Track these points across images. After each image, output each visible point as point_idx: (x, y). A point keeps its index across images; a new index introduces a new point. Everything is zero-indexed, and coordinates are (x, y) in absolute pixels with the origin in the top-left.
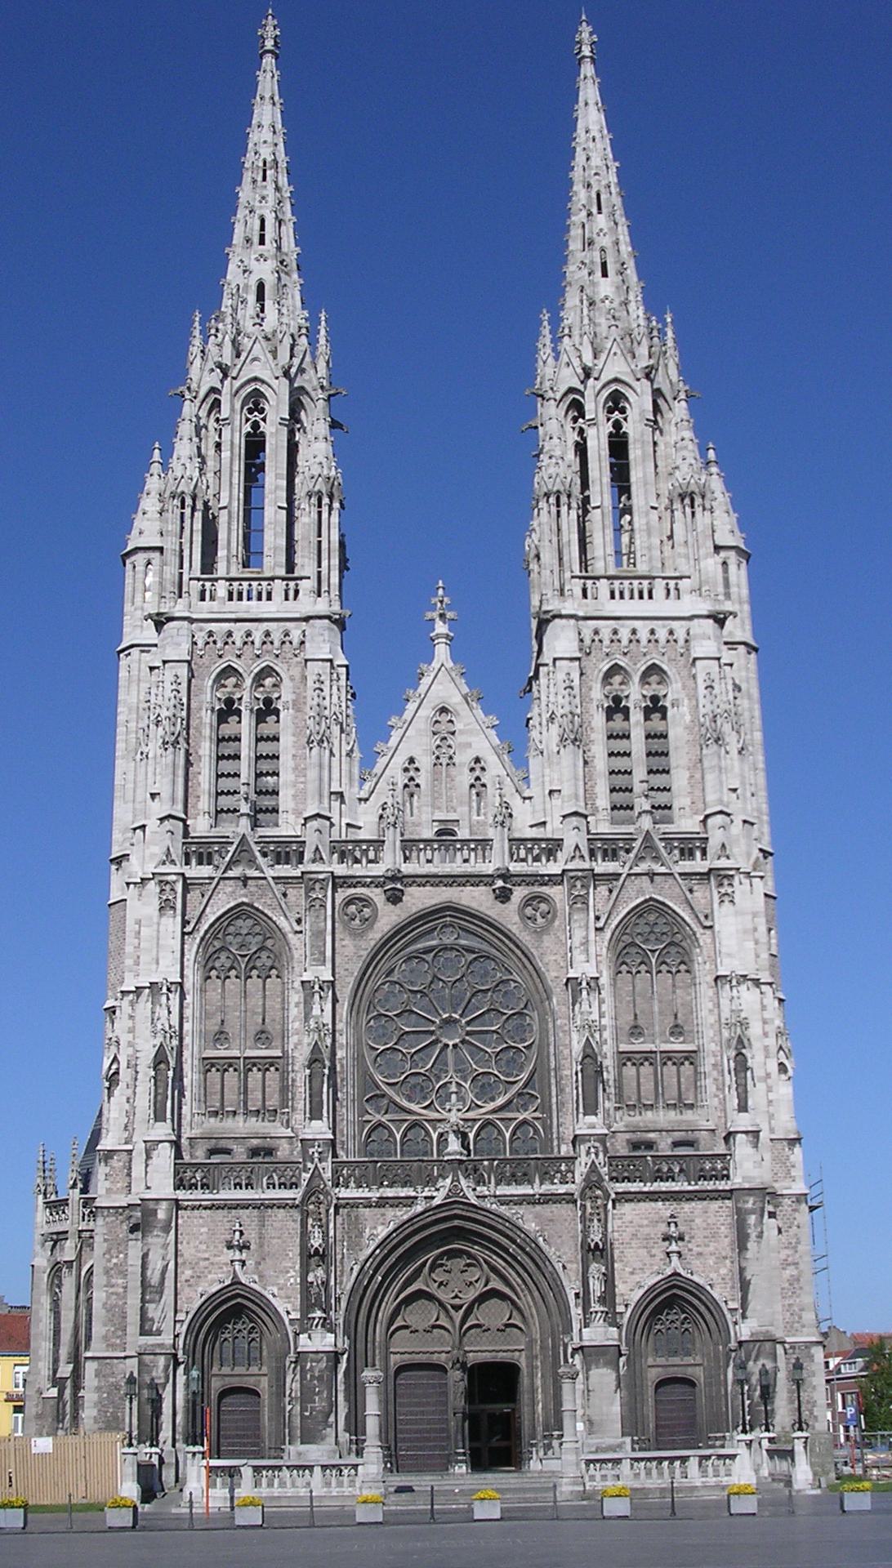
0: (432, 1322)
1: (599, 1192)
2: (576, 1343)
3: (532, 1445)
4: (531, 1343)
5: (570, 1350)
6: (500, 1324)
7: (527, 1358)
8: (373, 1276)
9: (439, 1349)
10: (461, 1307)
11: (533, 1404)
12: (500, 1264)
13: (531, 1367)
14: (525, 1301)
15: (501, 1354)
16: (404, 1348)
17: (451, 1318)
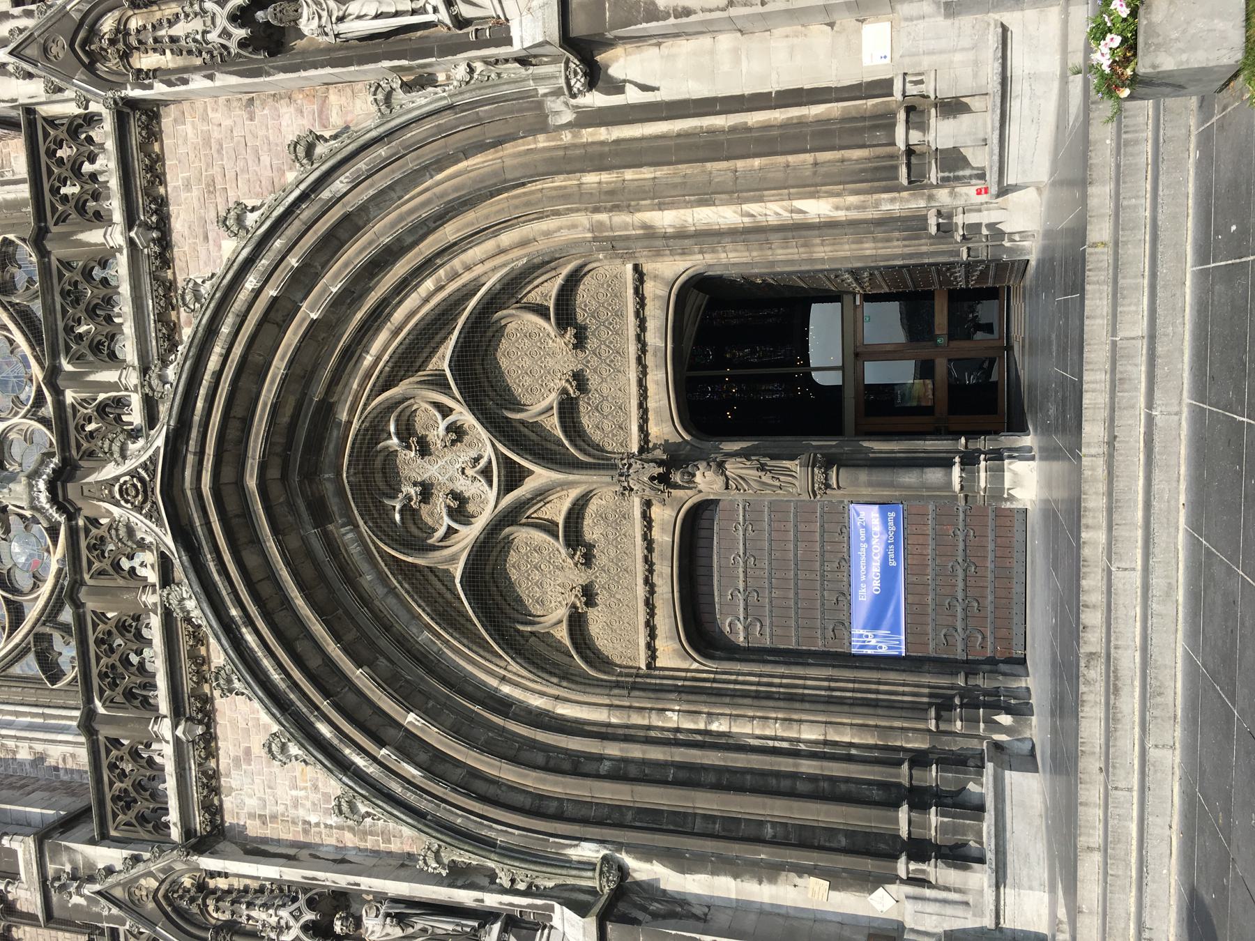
0: (560, 545)
1: (108, 25)
2: (556, 70)
3: (945, 230)
4: (615, 245)
5: (596, 99)
6: (558, 344)
7: (657, 254)
8: (409, 746)
9: (633, 527)
10: (506, 463)
11: (799, 230)
12: (381, 348)
13: (683, 239)
14: (483, 266)
15: (654, 338)
16: (635, 624)
17: (541, 495)
